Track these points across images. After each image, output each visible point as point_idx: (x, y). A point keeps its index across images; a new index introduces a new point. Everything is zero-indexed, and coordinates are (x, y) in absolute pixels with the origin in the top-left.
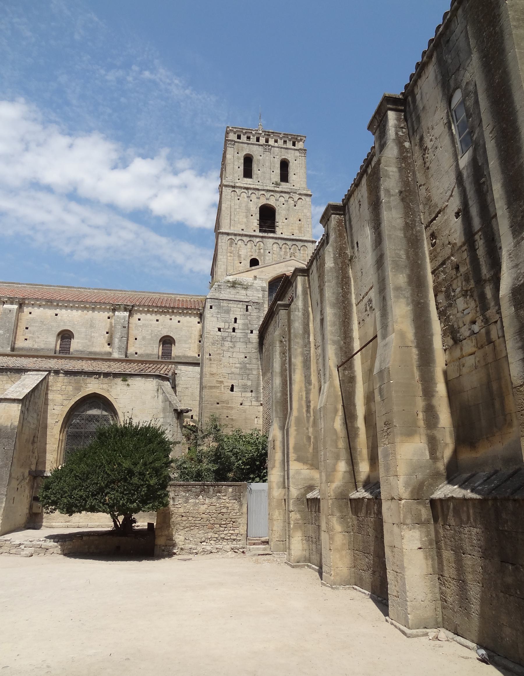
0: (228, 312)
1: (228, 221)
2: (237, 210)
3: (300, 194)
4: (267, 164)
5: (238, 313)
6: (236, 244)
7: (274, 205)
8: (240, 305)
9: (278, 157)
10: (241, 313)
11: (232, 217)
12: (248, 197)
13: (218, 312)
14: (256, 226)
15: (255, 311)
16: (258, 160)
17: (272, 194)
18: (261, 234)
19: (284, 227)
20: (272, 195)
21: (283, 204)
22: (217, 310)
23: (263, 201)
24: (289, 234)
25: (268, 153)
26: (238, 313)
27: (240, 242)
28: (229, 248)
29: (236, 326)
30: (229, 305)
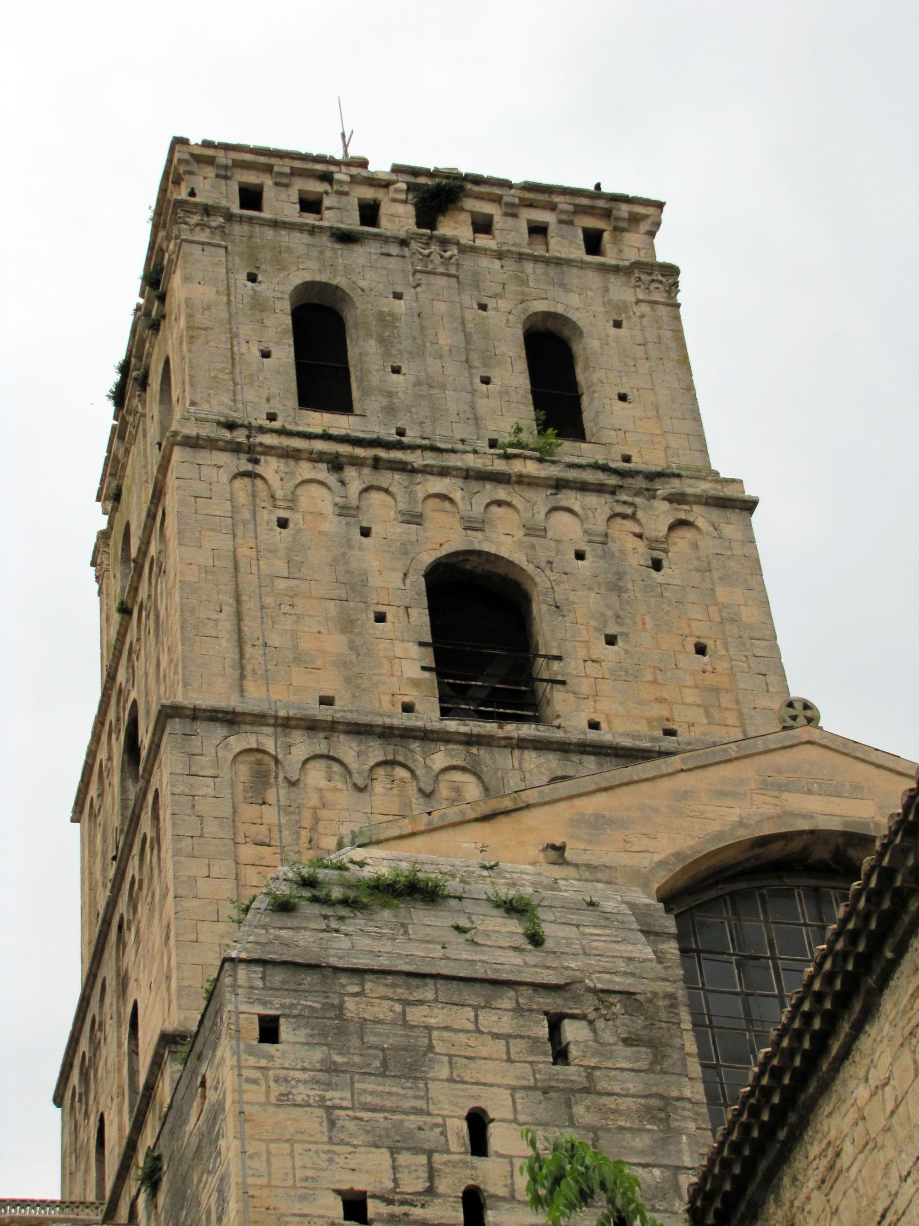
0: (408, 1062)
1: (226, 645)
2: (281, 584)
3: (678, 499)
4: (446, 339)
5: (489, 1071)
6: (293, 784)
7: (519, 558)
8: (500, 1018)
9: (504, 305)
10: (518, 1074)
11: (251, 627)
12: (345, 511)
13: (331, 1068)
15: (623, 1057)
16: (387, 320)
17: (501, 493)
18: (452, 725)
19: (605, 686)
20: (499, 503)
21: (580, 556)
22: (318, 1055)
23: (444, 537)
24: (642, 728)
25: (442, 281)
26: (489, 1071)
27: (316, 775)
28: (248, 812)
29: (491, 1174)
30: (415, 1015)
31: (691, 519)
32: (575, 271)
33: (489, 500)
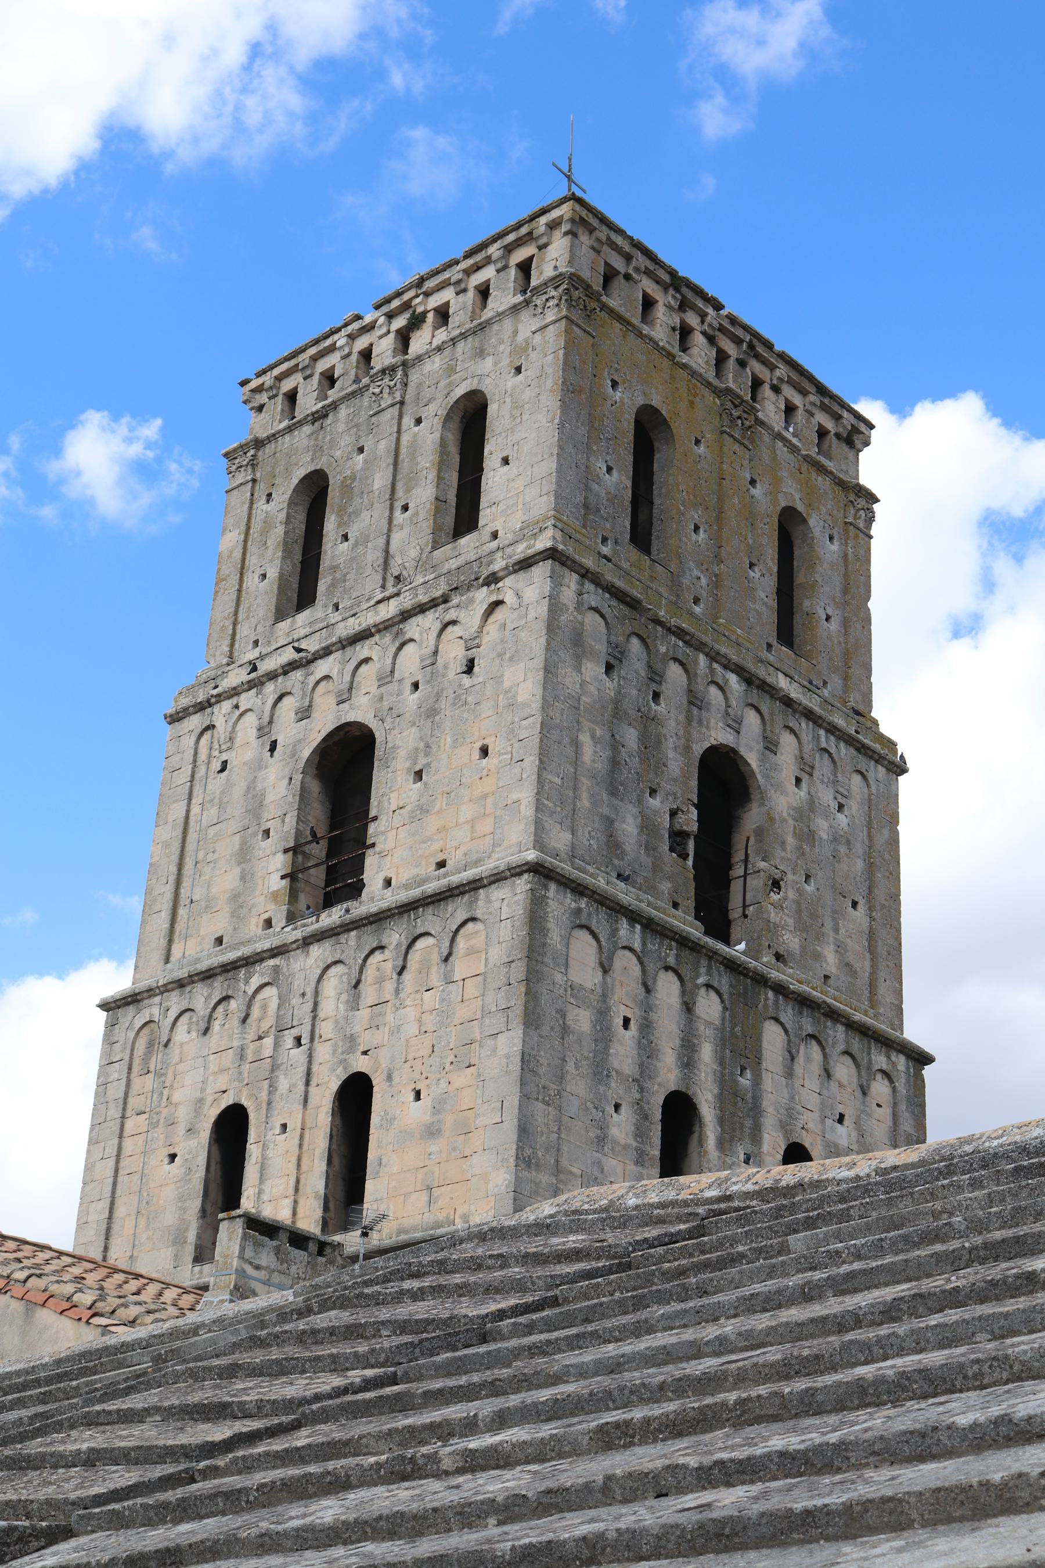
2: (211, 832)
9: (432, 408)
14: (275, 896)
23: (326, 719)
31: (500, 598)
32: (495, 327)
33: (356, 663)
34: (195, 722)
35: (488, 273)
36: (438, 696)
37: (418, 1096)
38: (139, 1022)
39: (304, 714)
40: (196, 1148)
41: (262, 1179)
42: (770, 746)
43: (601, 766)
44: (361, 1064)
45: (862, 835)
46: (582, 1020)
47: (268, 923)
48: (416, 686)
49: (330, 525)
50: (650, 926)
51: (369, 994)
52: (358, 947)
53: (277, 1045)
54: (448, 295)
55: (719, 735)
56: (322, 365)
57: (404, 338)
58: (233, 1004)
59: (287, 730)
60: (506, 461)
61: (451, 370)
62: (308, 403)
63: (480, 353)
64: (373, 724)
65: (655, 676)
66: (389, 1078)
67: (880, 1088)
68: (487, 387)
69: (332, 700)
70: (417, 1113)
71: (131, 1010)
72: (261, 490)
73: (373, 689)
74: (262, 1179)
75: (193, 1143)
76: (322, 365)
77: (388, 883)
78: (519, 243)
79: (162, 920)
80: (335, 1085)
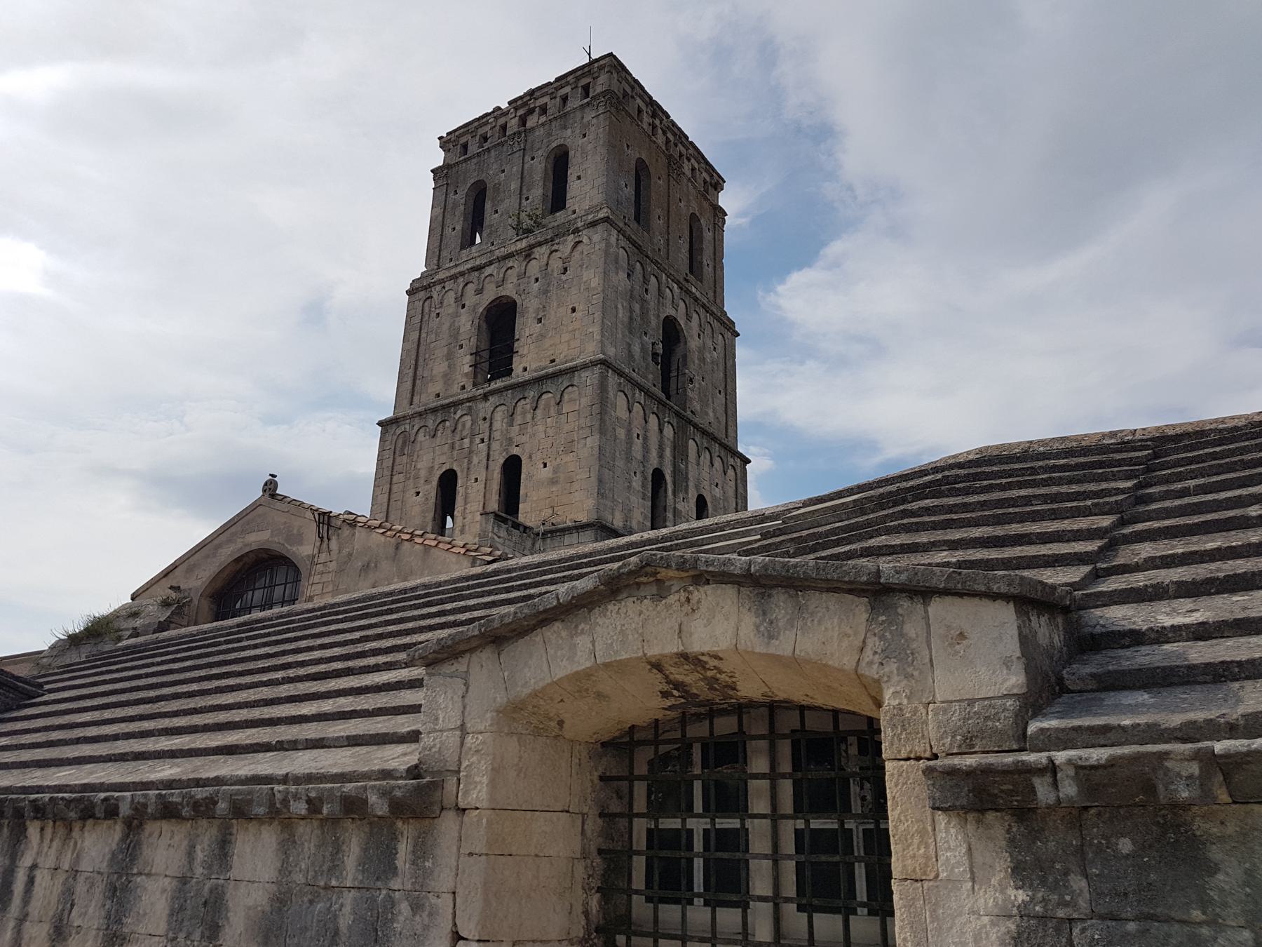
23: (490, 294)
34: (422, 294)
35: (567, 89)
36: (549, 284)
37: (545, 465)
38: (398, 432)
39: (479, 292)
40: (430, 490)
41: (466, 503)
42: (689, 318)
43: (626, 320)
44: (516, 451)
45: (722, 361)
46: (621, 433)
47: (463, 387)
48: (537, 280)
49: (488, 206)
50: (647, 393)
51: (518, 419)
52: (513, 398)
53: (471, 442)
54: (546, 99)
55: (672, 312)
56: (481, 131)
57: (523, 121)
58: (448, 423)
59: (470, 299)
60: (579, 178)
61: (550, 135)
62: (473, 148)
63: (565, 127)
64: (515, 297)
65: (646, 281)
66: (530, 457)
67: (731, 472)
68: (568, 142)
69: (493, 286)
70: (546, 473)
71: (394, 426)
72: (451, 189)
73: (515, 280)
74: (466, 503)
75: (428, 487)
76: (481, 131)
77: (525, 369)
78: (583, 76)
79: (409, 385)
80: (502, 461)
